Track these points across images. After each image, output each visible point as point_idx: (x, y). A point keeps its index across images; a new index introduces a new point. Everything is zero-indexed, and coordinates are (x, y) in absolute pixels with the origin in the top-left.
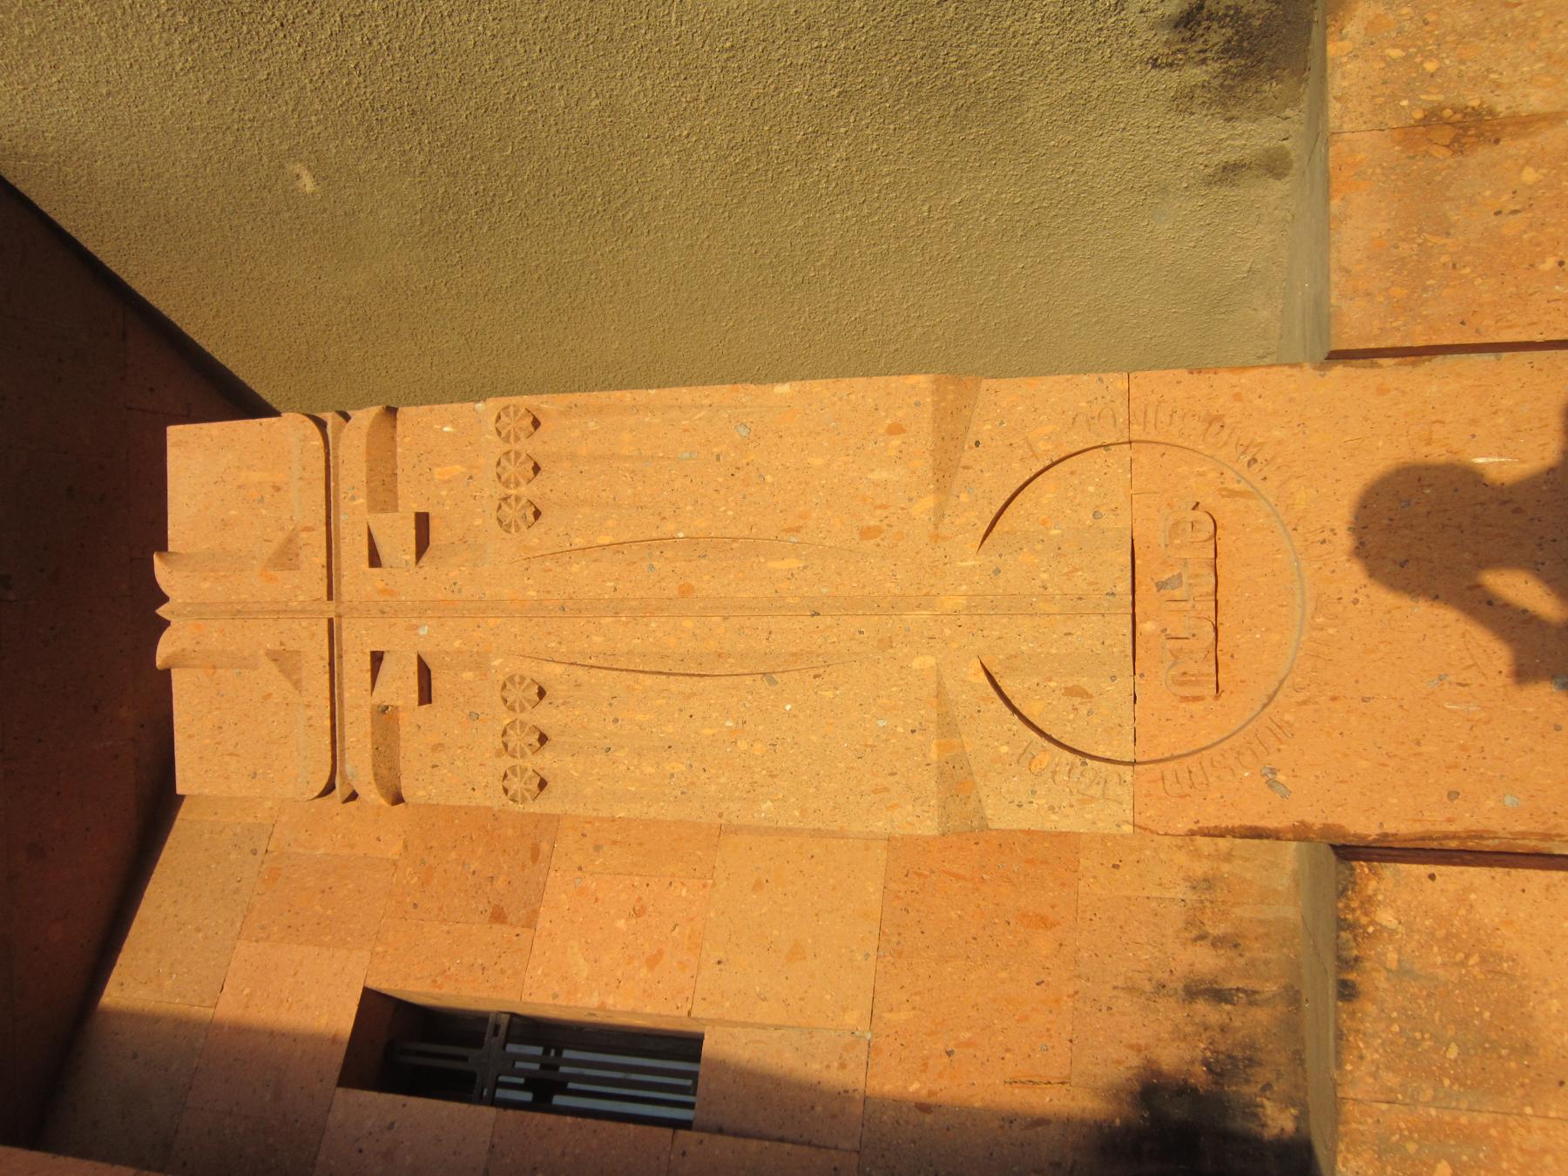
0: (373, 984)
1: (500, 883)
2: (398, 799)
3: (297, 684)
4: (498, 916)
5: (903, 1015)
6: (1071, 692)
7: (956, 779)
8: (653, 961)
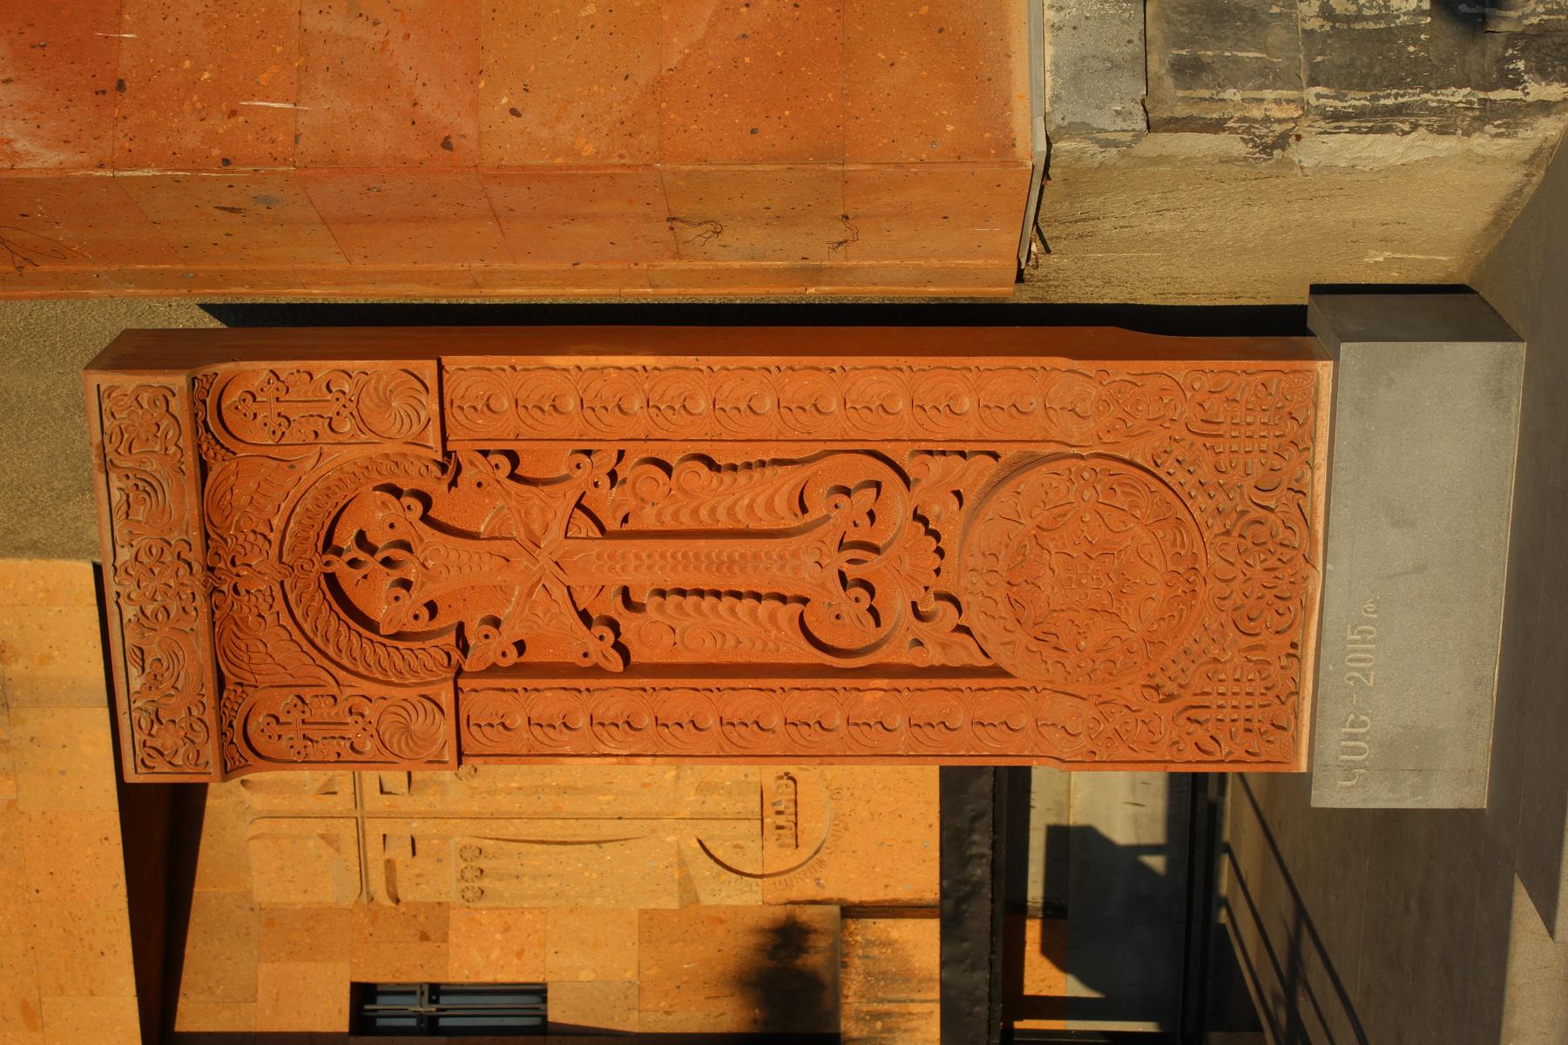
0: (356, 979)
1: (421, 918)
2: (398, 901)
3: (337, 850)
4: (424, 937)
5: (654, 972)
6: (736, 847)
7: (686, 885)
8: (520, 955)
